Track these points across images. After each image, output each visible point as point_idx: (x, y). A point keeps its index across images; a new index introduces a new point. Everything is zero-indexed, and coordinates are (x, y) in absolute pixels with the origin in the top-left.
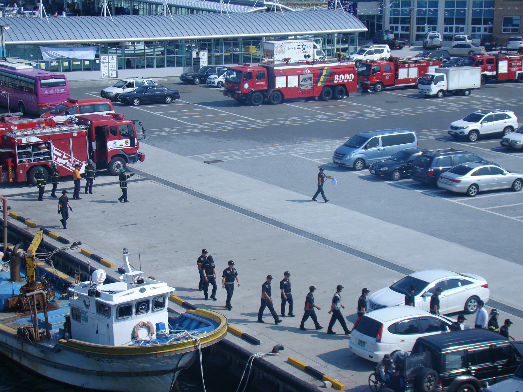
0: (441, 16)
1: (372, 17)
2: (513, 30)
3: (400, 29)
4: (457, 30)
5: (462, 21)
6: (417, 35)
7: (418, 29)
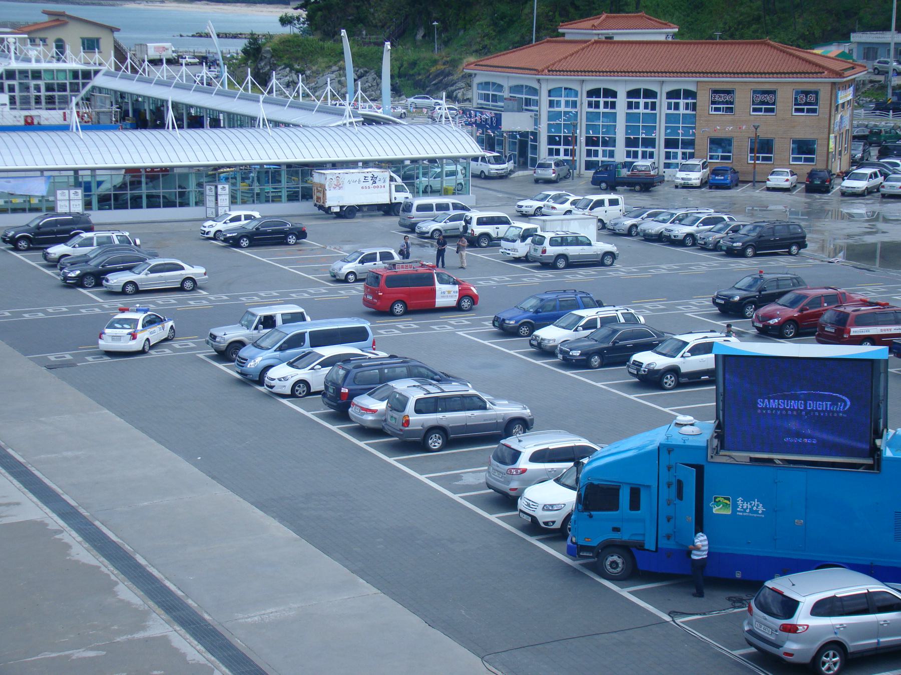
0: (620, 136)
1: (524, 135)
2: (723, 158)
4: (644, 156)
5: (650, 143)
7: (589, 153)
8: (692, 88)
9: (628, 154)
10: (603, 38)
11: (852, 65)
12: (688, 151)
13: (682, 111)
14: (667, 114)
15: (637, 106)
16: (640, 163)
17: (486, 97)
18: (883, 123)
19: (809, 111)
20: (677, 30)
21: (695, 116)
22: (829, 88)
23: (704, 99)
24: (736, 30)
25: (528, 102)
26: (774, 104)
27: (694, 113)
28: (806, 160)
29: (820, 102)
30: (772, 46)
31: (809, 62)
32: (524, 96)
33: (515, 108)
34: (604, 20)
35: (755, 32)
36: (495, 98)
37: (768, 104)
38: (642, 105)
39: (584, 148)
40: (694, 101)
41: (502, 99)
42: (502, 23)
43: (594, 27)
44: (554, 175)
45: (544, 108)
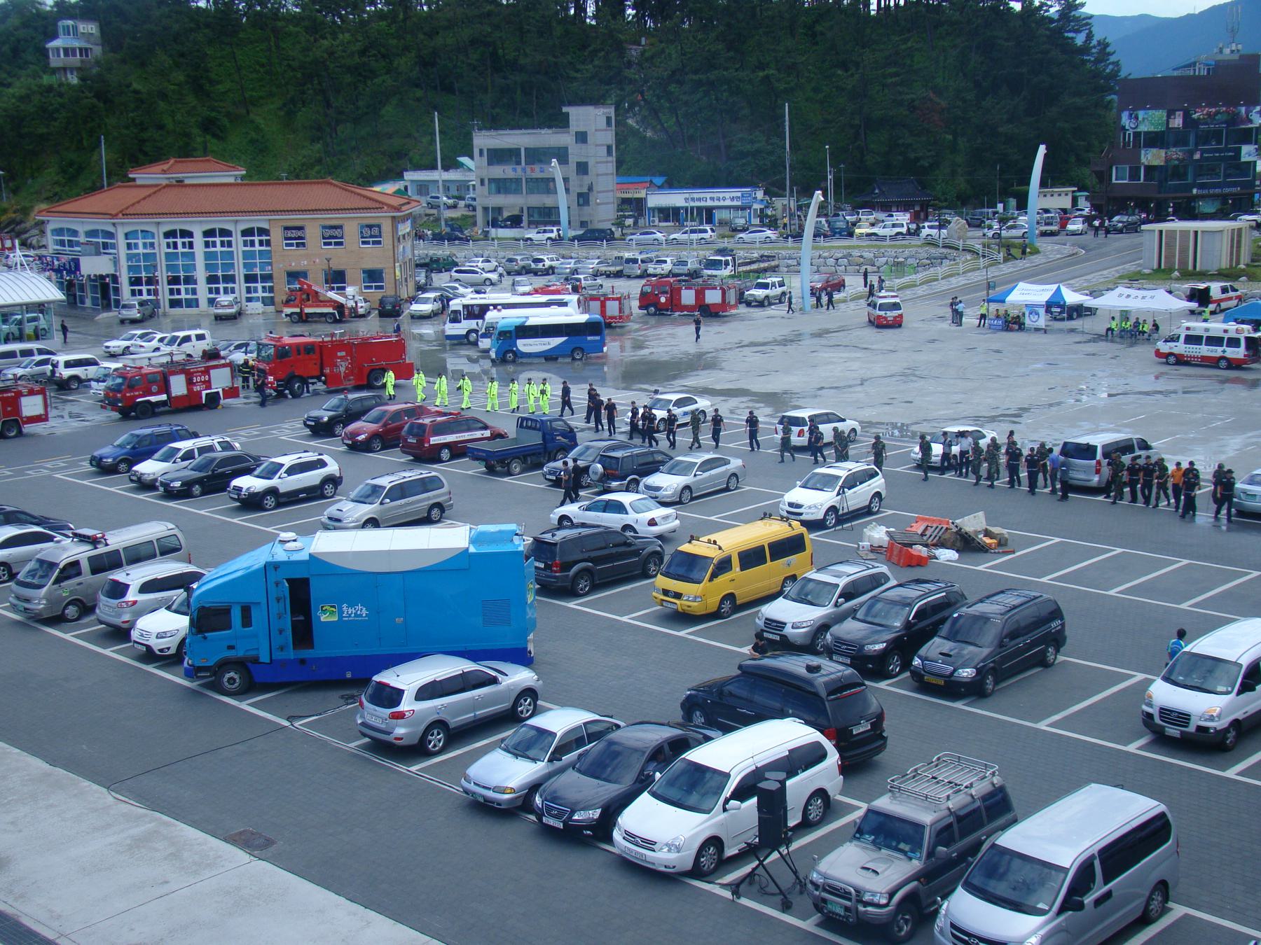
0: (201, 274)
3: (145, 292)
4: (226, 291)
5: (230, 279)
6: (171, 301)
8: (266, 226)
9: (210, 291)
10: (174, 183)
11: (407, 201)
12: (267, 285)
13: (257, 248)
14: (244, 251)
15: (214, 245)
16: (224, 299)
17: (62, 243)
18: (441, 252)
19: (374, 243)
20: (245, 172)
21: (270, 251)
22: (389, 222)
23: (277, 236)
24: (301, 171)
25: (105, 246)
26: (342, 238)
27: (268, 248)
28: (377, 288)
29: (384, 234)
30: (335, 185)
31: (371, 199)
32: (101, 240)
33: (93, 252)
34: (172, 165)
35: (318, 172)
36: (71, 244)
37: (336, 237)
38: (218, 244)
39: (167, 287)
40: (268, 238)
41: (78, 244)
42: (71, 170)
43: (164, 172)
44: (138, 315)
45: (123, 251)
